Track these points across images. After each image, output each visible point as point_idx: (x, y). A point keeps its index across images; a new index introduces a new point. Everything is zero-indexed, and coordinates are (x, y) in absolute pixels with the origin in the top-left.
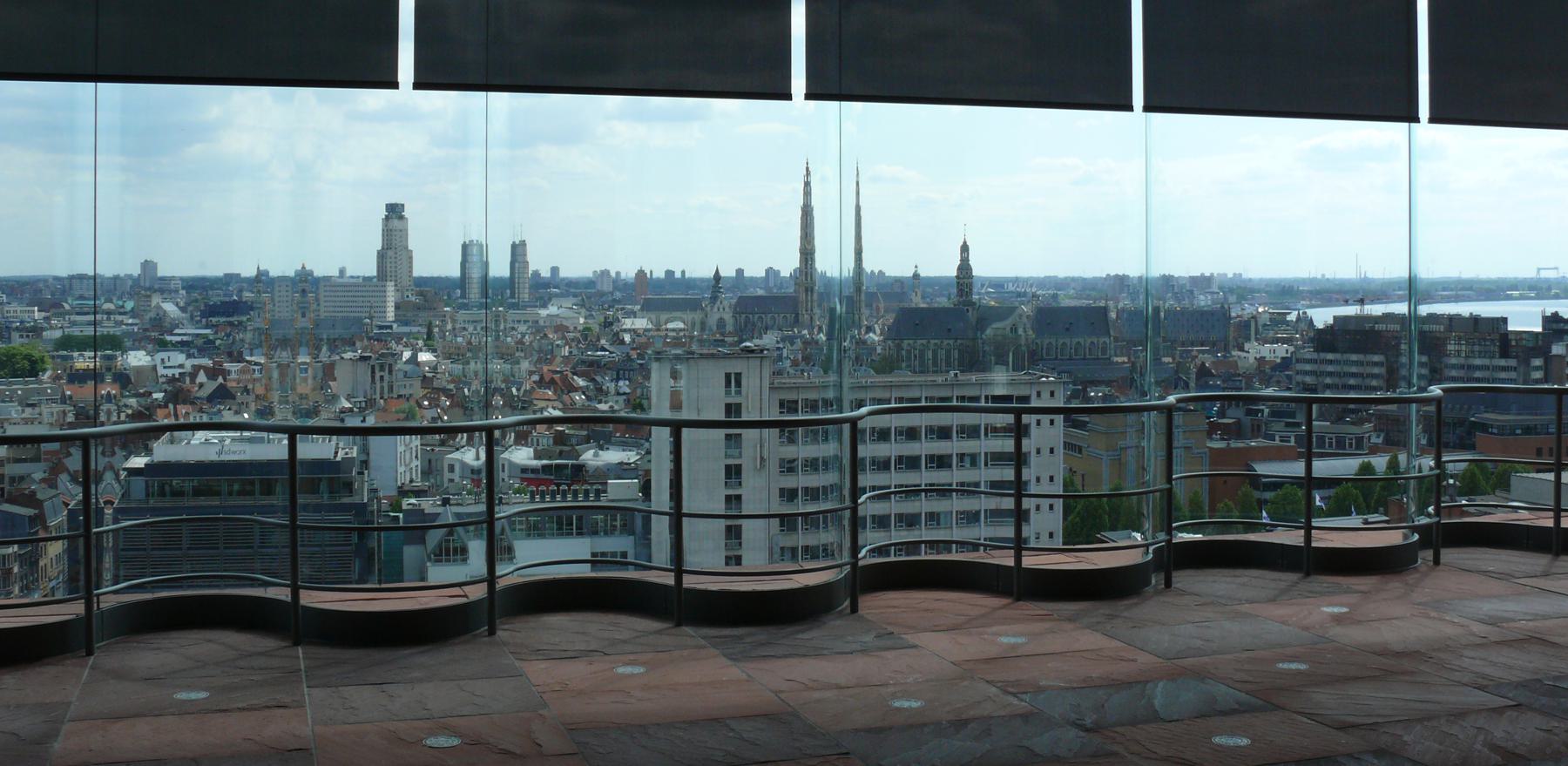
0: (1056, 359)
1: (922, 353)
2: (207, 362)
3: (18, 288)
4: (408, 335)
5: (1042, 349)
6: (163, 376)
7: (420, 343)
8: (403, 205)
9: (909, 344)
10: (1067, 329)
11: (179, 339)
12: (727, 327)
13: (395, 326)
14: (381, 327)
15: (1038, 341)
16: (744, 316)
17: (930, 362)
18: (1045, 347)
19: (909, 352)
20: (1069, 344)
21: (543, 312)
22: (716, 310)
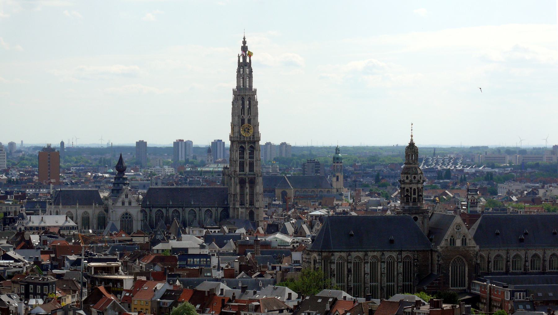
0: (507, 273)
1: (357, 265)
5: (489, 262)
9: (341, 257)
10: (521, 240)
15: (484, 254)
16: (155, 210)
17: (368, 277)
19: (340, 266)
20: (523, 257)
22: (119, 204)
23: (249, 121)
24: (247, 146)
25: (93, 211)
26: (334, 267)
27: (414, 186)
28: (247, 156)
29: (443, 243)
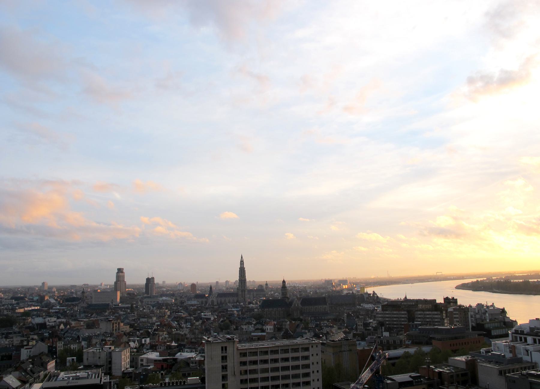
2: (64, 320)
3: (5, 291)
4: (124, 308)
6: (48, 325)
7: (129, 311)
8: (123, 269)
9: (267, 310)
11: (54, 311)
12: (215, 303)
13: (120, 304)
14: (115, 305)
18: (305, 309)
21: (161, 299)
23: (243, 276)
24: (243, 282)
25: (204, 300)
26: (265, 313)
27: (285, 291)
28: (243, 284)
29: (293, 306)
